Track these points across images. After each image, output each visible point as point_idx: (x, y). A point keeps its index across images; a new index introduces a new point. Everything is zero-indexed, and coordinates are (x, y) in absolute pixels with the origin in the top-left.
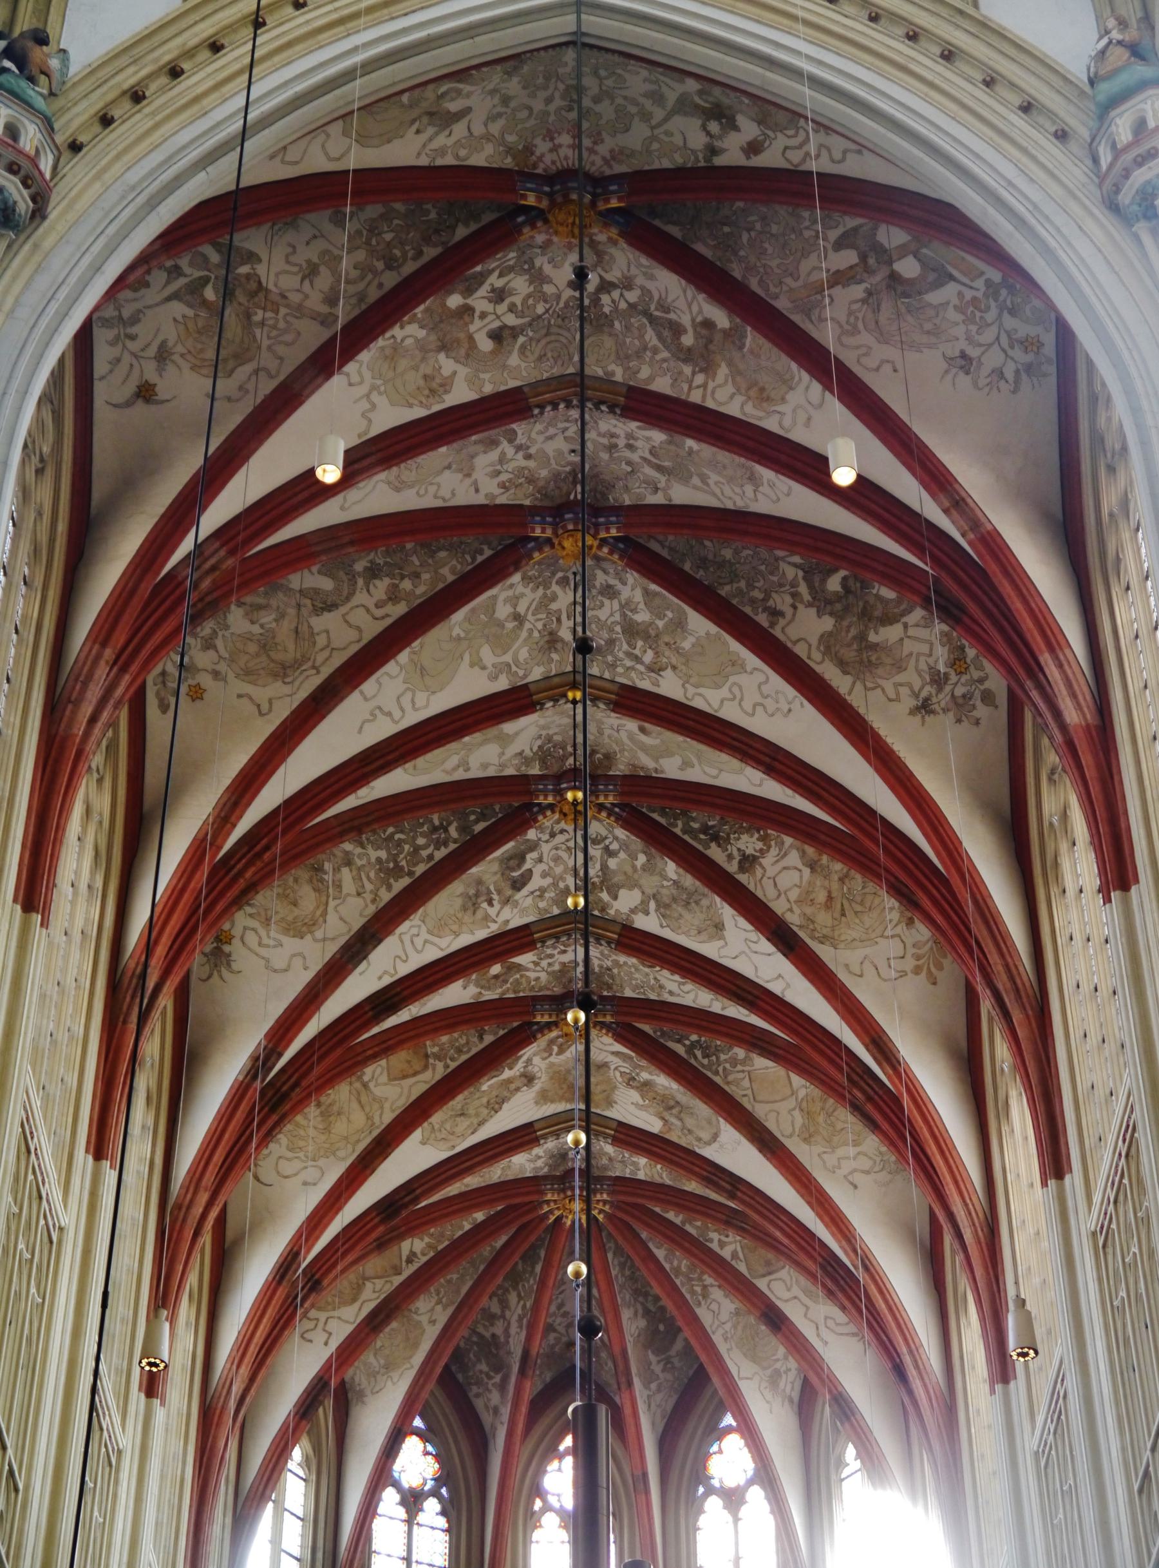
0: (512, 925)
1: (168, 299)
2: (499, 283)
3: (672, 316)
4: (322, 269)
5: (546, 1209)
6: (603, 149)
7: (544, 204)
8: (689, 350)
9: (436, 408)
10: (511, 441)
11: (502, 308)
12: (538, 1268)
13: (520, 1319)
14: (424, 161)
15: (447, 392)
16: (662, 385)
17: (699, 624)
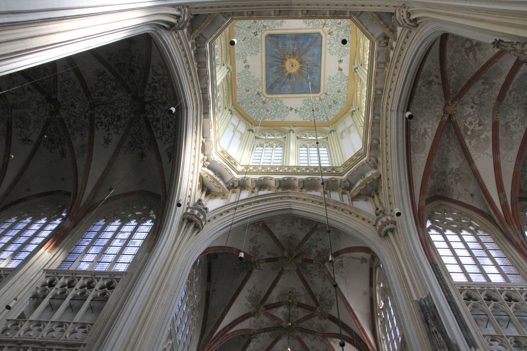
1: (456, 186)
2: (468, 123)
3: (481, 90)
4: (457, 156)
7: (448, 115)
9: (491, 140)
10: (510, 122)
11: (474, 123)
14: (433, 138)
15: (489, 137)
16: (497, 93)
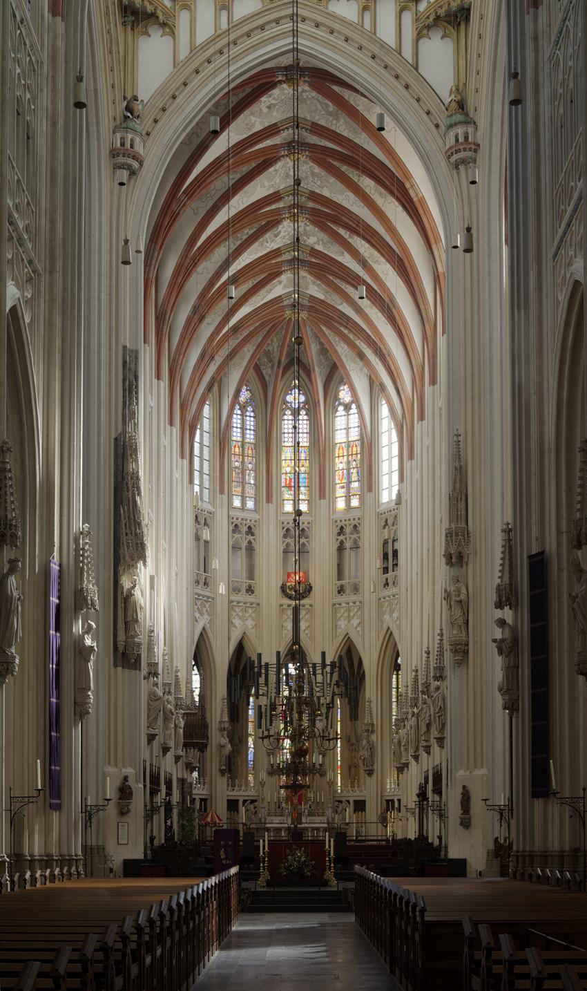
0: (274, 248)
5: (286, 315)
8: (331, 112)
12: (284, 332)
13: (278, 347)
16: (322, 122)
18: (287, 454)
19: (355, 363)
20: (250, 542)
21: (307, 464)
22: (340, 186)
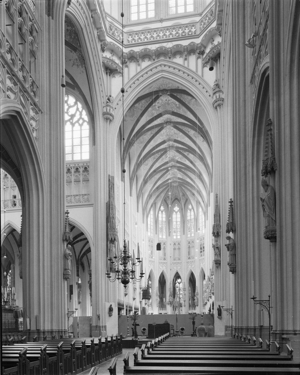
6: (167, 86)
16: (175, 111)
17: (181, 134)
18: (174, 223)
19: (192, 197)
20: (164, 247)
21: (180, 226)
22: (183, 136)
